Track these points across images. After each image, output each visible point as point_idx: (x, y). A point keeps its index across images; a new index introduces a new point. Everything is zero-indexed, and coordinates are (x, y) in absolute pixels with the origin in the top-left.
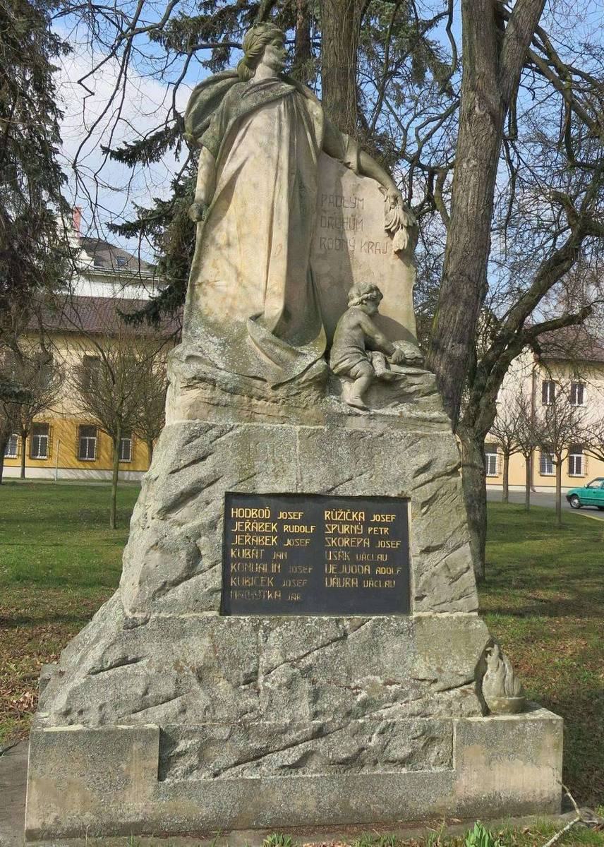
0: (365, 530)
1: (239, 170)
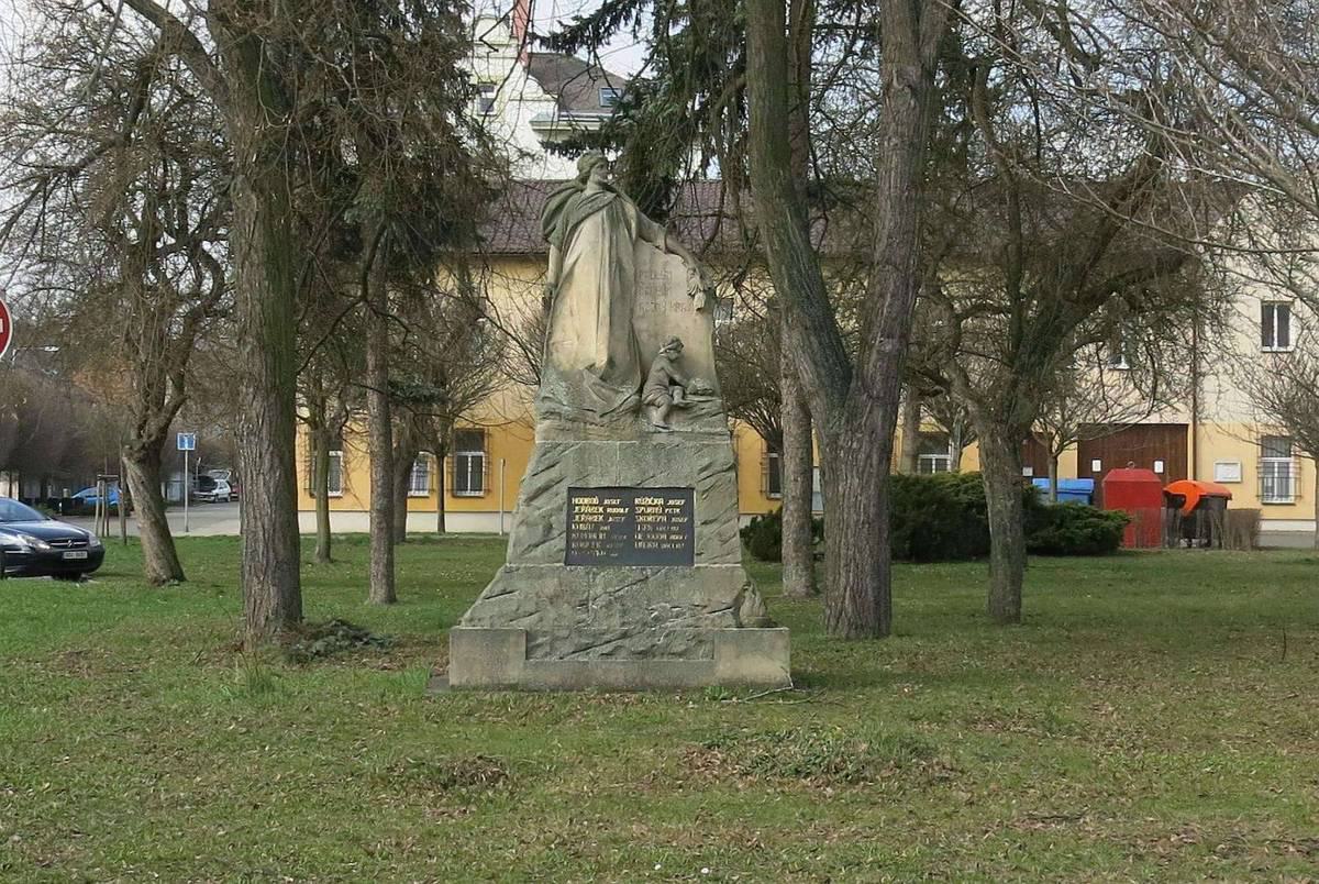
0: (663, 510)
1: (575, 263)
